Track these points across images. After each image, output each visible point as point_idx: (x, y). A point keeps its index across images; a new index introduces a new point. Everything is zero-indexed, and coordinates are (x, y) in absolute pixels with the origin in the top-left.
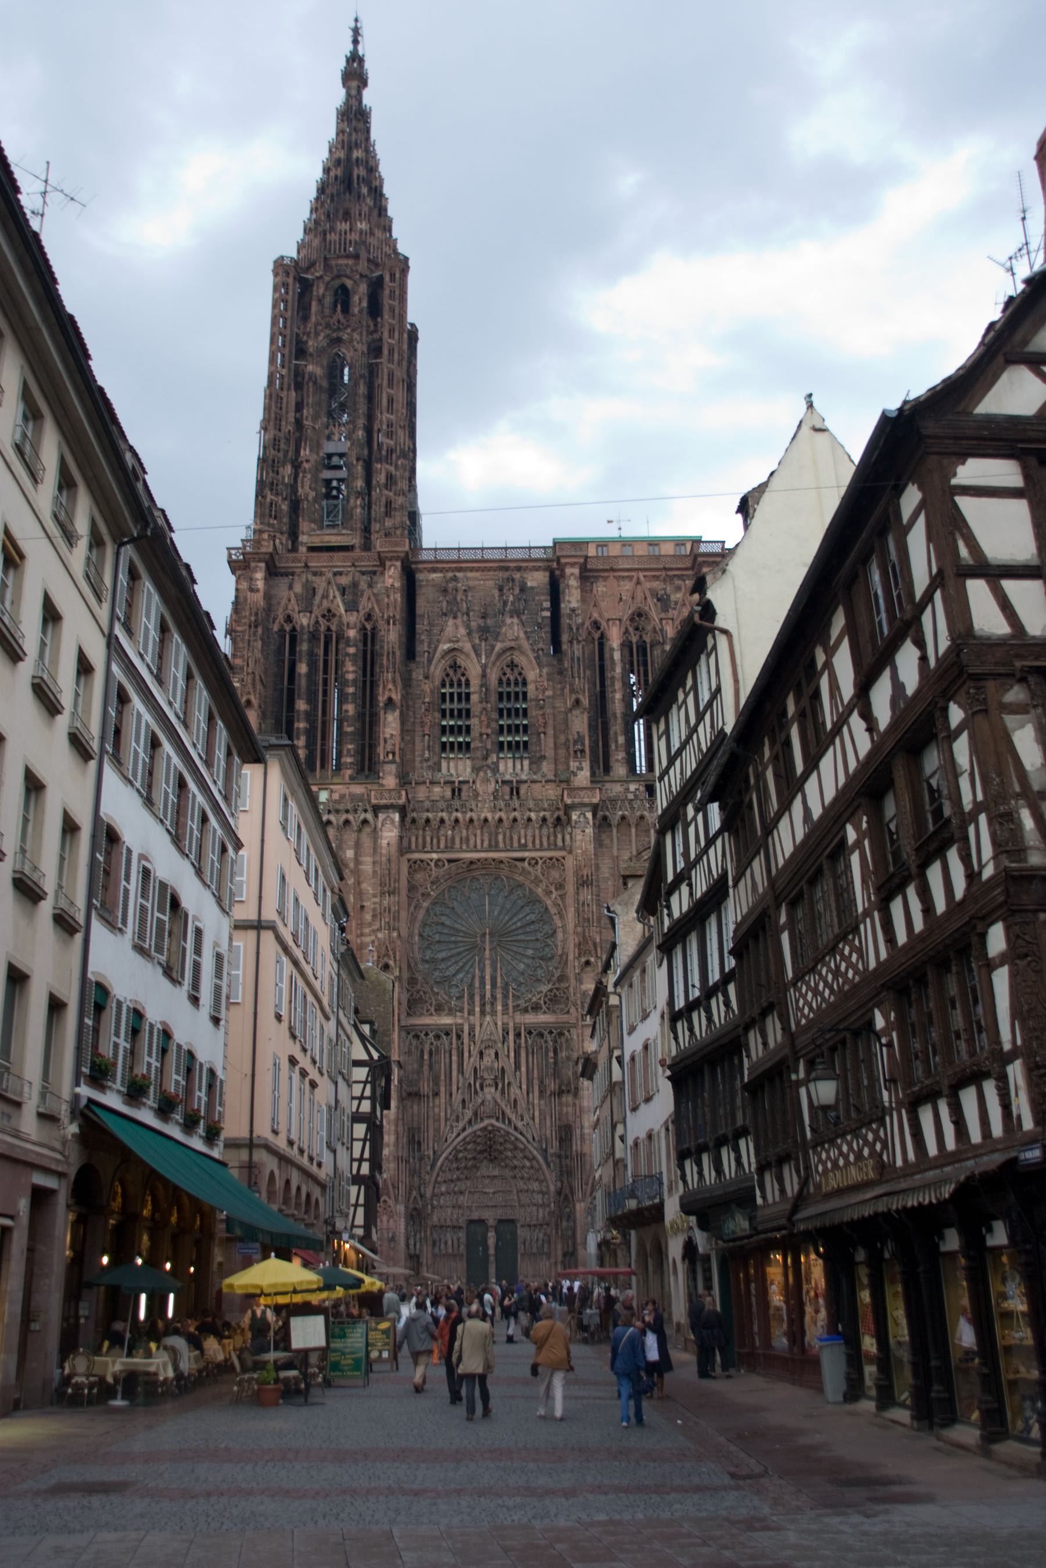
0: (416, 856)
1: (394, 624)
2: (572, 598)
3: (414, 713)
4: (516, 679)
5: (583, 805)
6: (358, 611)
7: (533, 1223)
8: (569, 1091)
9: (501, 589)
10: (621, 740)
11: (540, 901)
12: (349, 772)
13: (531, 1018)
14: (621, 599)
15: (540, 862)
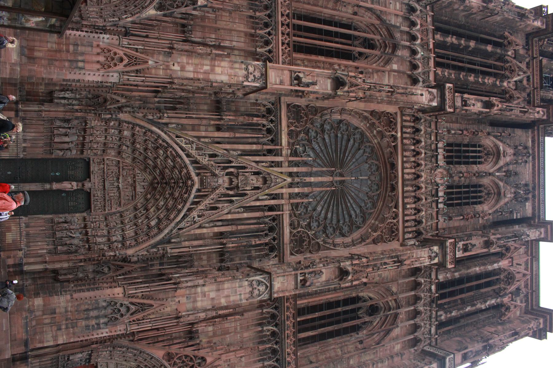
0: (399, 120)
1: (521, 112)
2: (533, 234)
3: (466, 124)
4: (482, 197)
5: (444, 255)
6: (515, 90)
7: (89, 230)
8: (222, 261)
9: (526, 185)
10: (457, 275)
11: (364, 221)
12: (440, 73)
13: (286, 221)
14: (521, 265)
15: (395, 221)
